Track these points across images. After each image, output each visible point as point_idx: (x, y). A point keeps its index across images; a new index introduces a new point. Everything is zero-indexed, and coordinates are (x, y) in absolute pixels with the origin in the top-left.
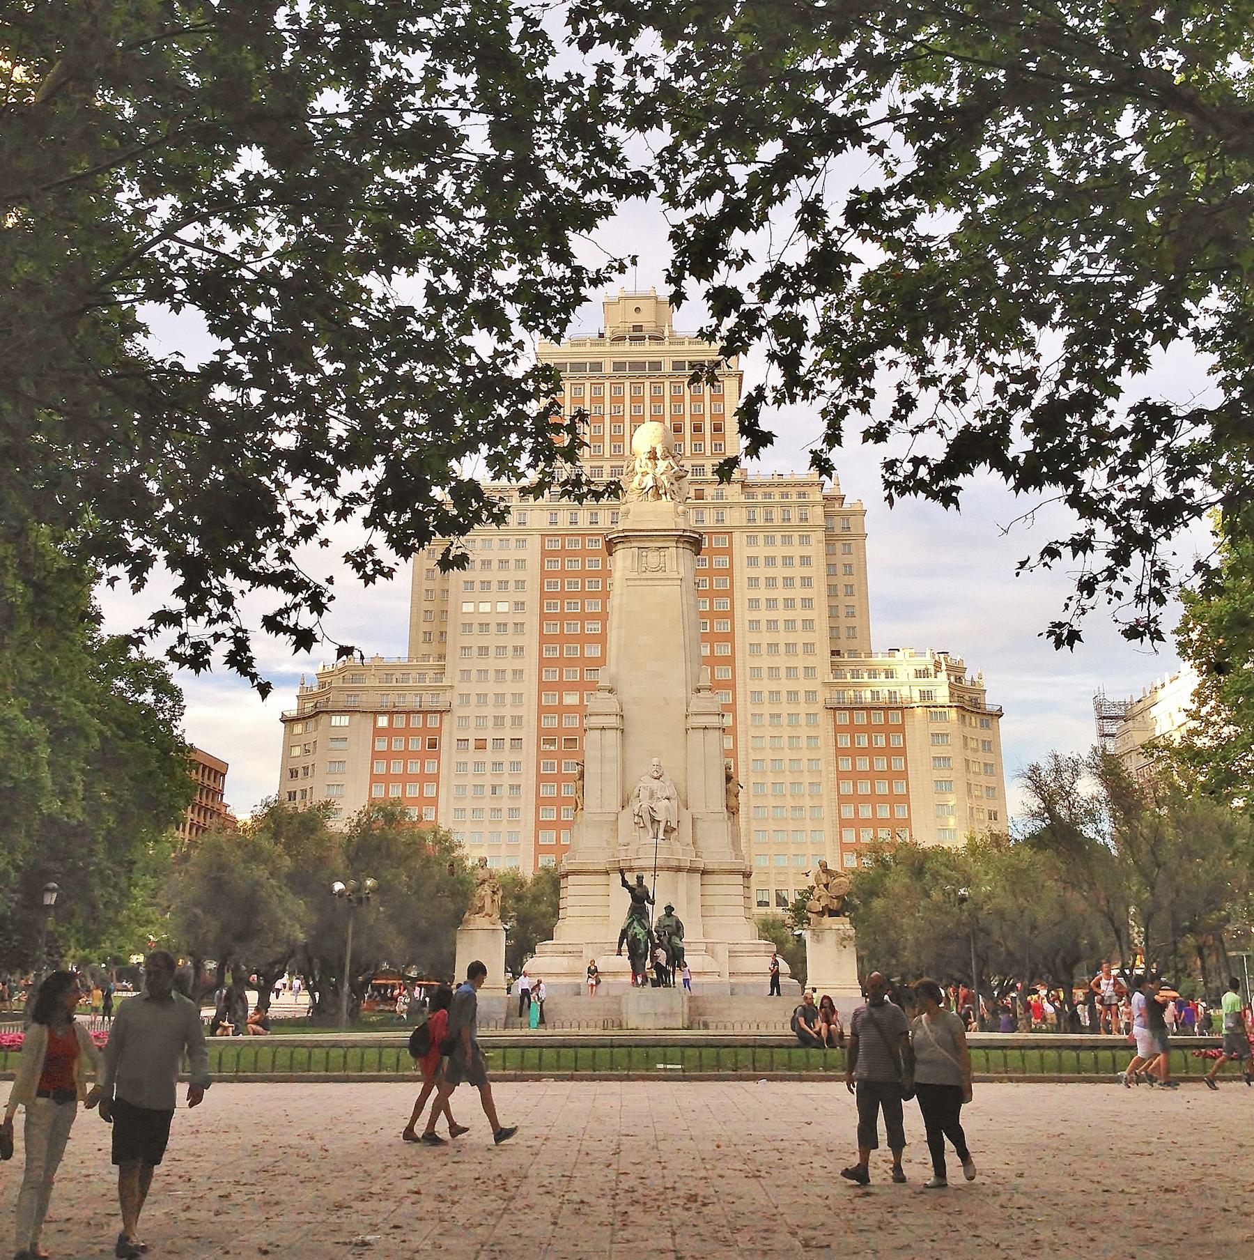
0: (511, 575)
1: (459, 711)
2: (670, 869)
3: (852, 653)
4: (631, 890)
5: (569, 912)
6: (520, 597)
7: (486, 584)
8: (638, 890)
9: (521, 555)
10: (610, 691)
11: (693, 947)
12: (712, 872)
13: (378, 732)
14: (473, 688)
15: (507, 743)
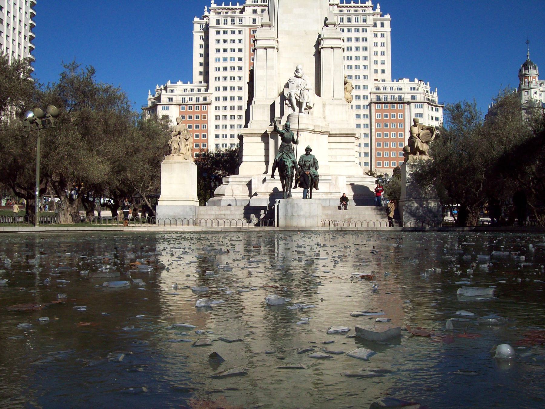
0: (236, 46)
1: (215, 103)
2: (308, 131)
3: (383, 80)
4: (282, 135)
5: (244, 159)
6: (240, 55)
7: (225, 50)
8: (286, 135)
9: (240, 37)
10: (270, 26)
11: (323, 178)
12: (335, 135)
13: (181, 113)
14: (221, 94)
15: (236, 117)
